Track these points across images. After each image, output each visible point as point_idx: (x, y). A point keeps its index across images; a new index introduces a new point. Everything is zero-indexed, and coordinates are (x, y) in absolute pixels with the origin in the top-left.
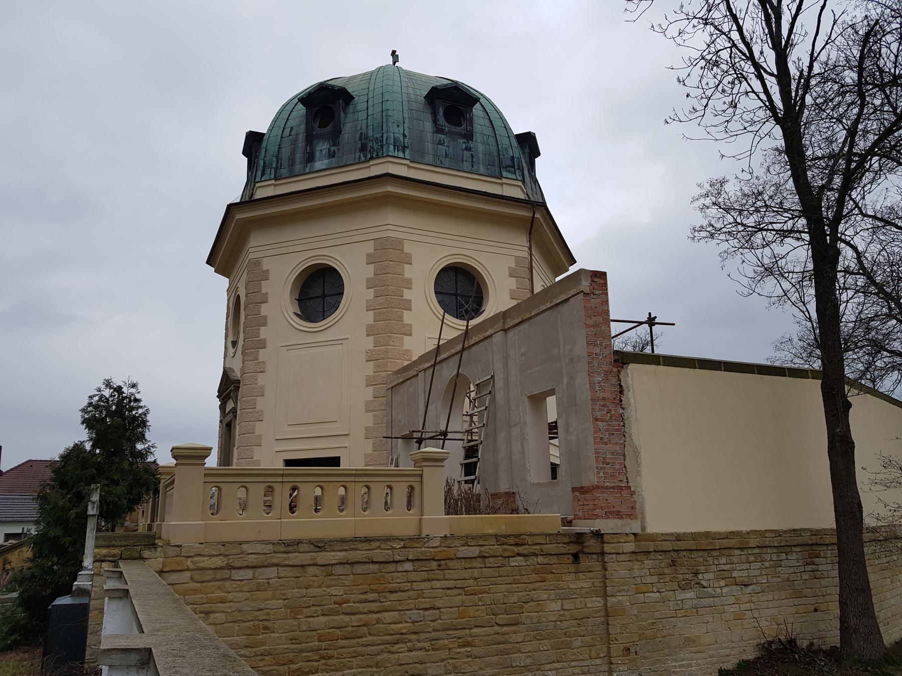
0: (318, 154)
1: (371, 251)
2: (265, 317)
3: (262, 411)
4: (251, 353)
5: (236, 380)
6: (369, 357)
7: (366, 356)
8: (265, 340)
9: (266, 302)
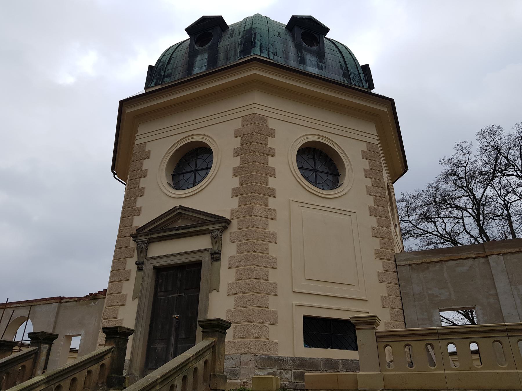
0: (308, 62)
3: (275, 258)
4: (259, 197)
7: (372, 232)
8: (274, 190)
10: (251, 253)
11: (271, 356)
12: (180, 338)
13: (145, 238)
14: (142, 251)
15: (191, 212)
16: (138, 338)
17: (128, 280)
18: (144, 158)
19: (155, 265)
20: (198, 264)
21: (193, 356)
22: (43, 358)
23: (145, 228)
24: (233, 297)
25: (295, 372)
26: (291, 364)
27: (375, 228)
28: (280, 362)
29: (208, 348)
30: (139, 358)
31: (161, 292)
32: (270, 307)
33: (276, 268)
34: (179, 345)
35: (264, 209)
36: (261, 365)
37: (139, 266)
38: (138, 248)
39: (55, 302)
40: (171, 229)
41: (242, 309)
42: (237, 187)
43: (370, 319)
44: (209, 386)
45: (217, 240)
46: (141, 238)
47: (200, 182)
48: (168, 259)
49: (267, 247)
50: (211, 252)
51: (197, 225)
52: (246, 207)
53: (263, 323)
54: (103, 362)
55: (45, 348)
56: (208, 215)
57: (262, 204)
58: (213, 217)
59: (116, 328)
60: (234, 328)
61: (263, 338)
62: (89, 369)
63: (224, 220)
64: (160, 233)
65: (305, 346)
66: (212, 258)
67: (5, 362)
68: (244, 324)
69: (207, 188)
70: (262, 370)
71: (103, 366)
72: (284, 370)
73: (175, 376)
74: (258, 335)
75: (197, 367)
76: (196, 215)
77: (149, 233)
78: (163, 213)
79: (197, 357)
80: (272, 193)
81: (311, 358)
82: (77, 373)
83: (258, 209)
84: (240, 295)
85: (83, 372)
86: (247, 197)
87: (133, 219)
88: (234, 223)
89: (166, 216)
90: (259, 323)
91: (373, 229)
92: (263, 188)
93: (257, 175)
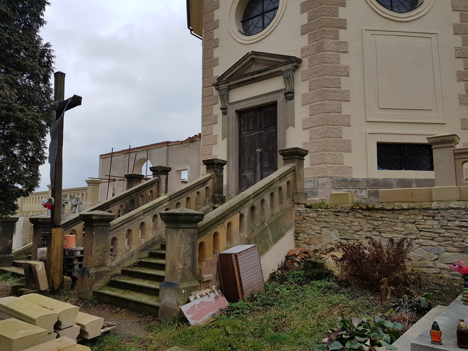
4: (329, 31)
5: (299, 59)
6: (459, 54)
7: (456, 52)
8: (345, 20)
10: (323, 89)
11: (346, 178)
12: (265, 168)
13: (225, 86)
14: (224, 97)
15: (263, 56)
16: (231, 168)
17: (216, 123)
18: (214, 9)
19: (237, 109)
20: (274, 104)
21: (277, 178)
22: (163, 185)
23: (224, 77)
24: (308, 130)
25: (369, 190)
26: (365, 185)
27: (459, 48)
28: (355, 183)
29: (289, 171)
30: (234, 183)
31: (244, 131)
32: (343, 137)
33: (349, 101)
34: (264, 173)
35: (335, 43)
36: (337, 186)
37: (224, 111)
38: (220, 95)
39: (164, 146)
40: (247, 75)
41: (317, 140)
42: (306, 23)
43: (448, 138)
44: (293, 201)
45: (289, 80)
46: (222, 87)
47: (269, 25)
48: (247, 102)
49: (339, 81)
50: (285, 92)
51: (270, 68)
52: (316, 43)
53: (338, 151)
54: (207, 185)
55: (163, 178)
56: (279, 56)
57: (332, 37)
58: (284, 58)
59: (213, 160)
60: (310, 156)
61: (338, 164)
62: (198, 190)
63: (295, 60)
64: (237, 79)
65: (378, 169)
66: (286, 98)
67: (138, 188)
68: (320, 153)
69: (275, 30)
70: (338, 190)
71: (207, 188)
72: (358, 189)
73: (264, 193)
74: (333, 161)
75: (281, 186)
76: (268, 58)
77: (228, 81)
78: (237, 61)
79: (281, 179)
80: (343, 25)
81: (385, 179)
82: (189, 193)
83: (329, 43)
84: (314, 128)
85: (194, 192)
86: (316, 32)
87: (212, 70)
88: (305, 61)
89: (240, 64)
90: (334, 151)
91: (456, 49)
92: (333, 20)
93: (326, 7)
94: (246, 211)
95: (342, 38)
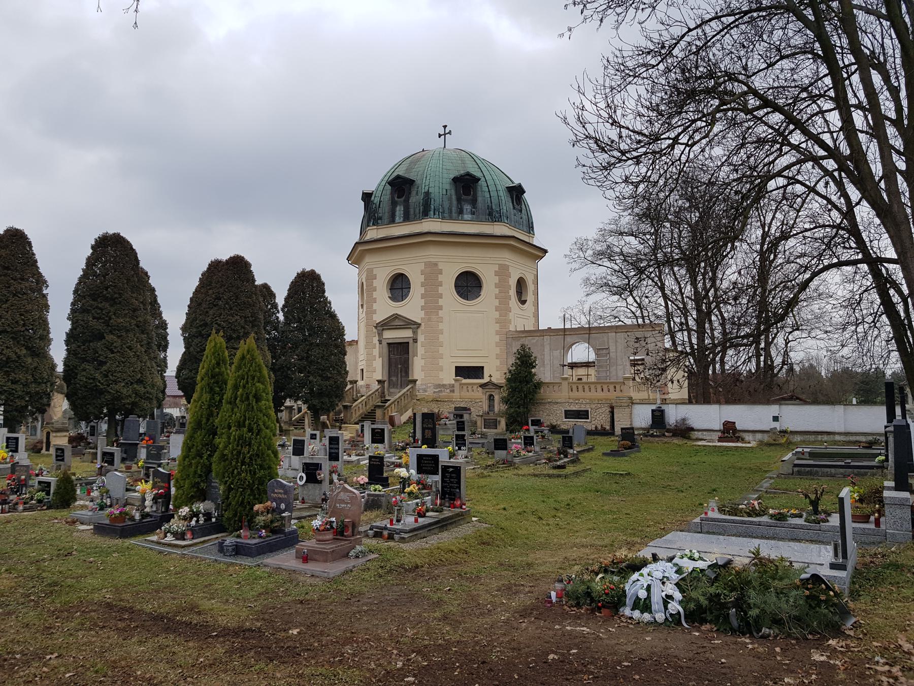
1: (497, 269)
2: (442, 294)
9: (441, 286)
14: (380, 335)
28: (444, 386)
45: (415, 333)
80: (441, 308)
88: (423, 324)
94: (396, 403)
95: (440, 315)
